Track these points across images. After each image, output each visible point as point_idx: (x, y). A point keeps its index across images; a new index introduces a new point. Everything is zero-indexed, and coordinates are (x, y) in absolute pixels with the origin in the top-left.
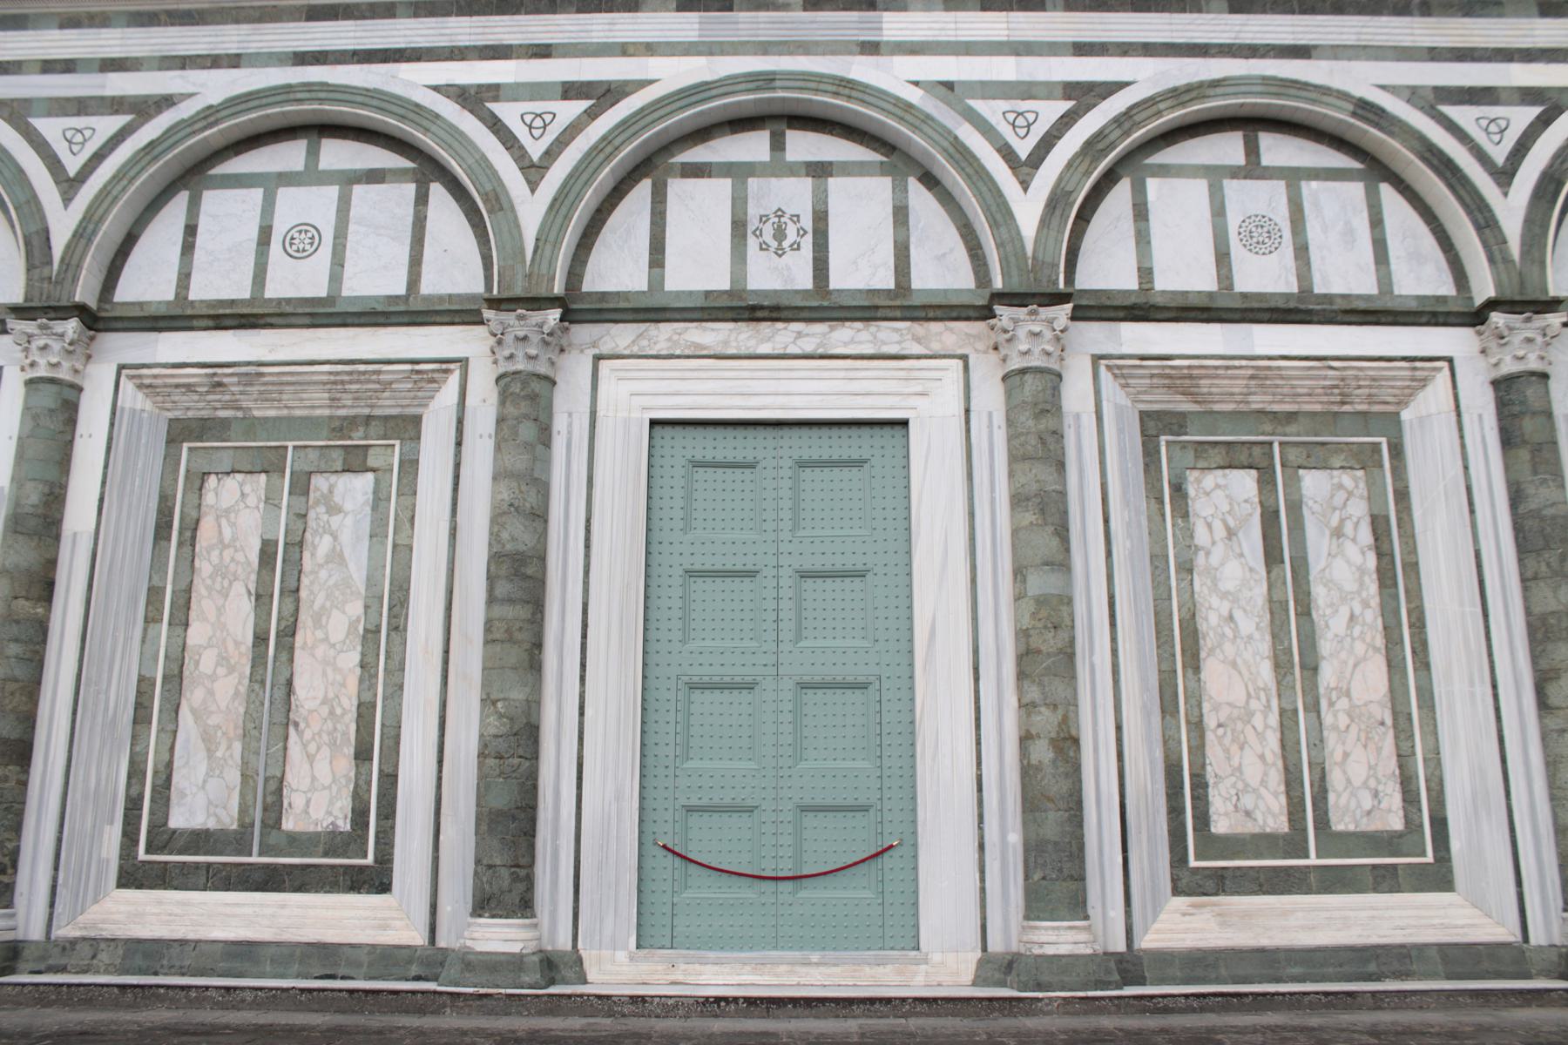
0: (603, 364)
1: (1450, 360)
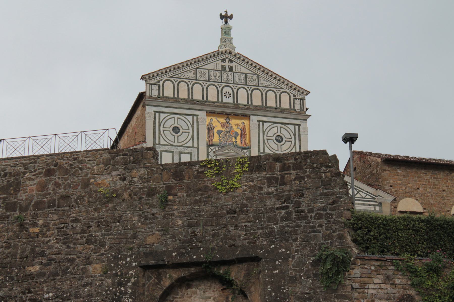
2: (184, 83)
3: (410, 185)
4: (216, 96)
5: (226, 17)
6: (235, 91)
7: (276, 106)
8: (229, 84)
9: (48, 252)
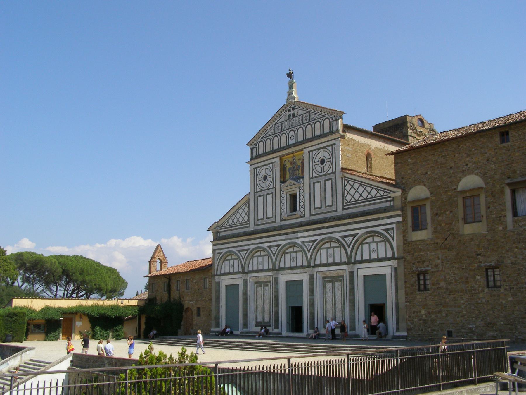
3: (419, 172)
5: (290, 75)
6: (296, 132)
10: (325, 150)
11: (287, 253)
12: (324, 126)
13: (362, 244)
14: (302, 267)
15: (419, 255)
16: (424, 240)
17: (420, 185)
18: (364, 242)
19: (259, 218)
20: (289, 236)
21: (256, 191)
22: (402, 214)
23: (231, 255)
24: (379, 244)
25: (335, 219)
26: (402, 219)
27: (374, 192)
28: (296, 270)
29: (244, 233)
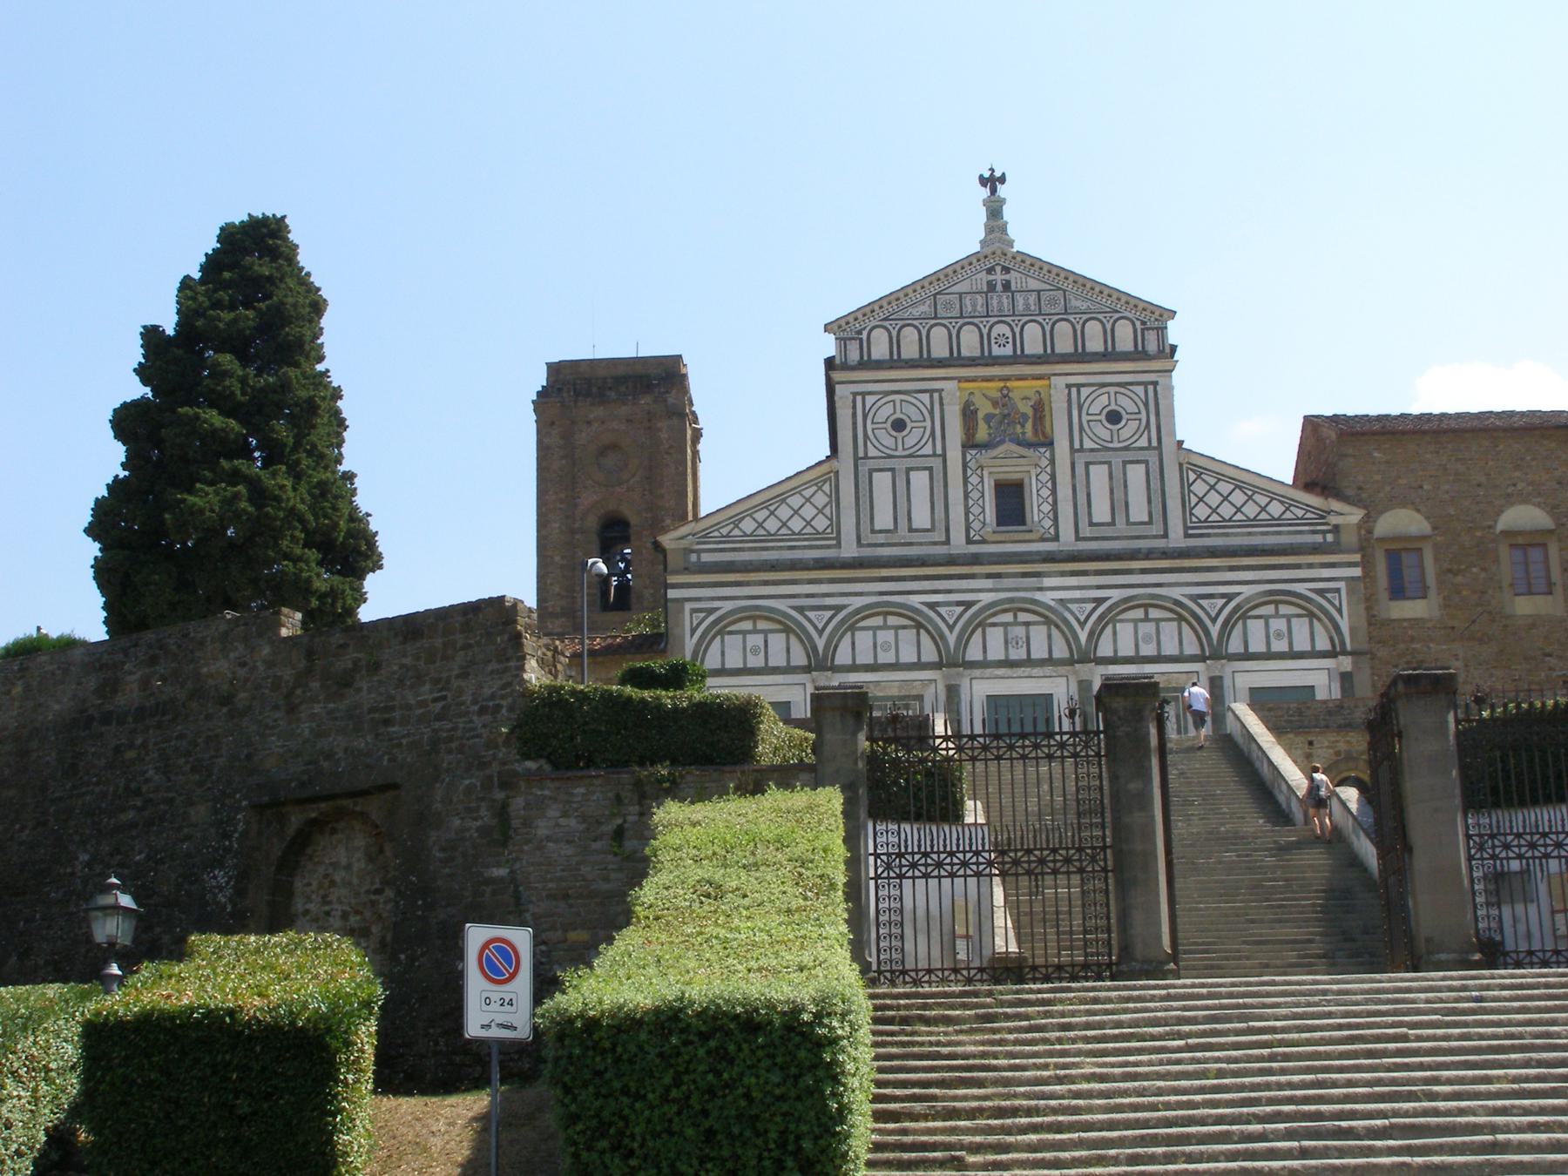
0: (973, 681)
1: (1197, 672)
2: (911, 328)
3: (1402, 481)
4: (978, 345)
5: (992, 182)
6: (1017, 330)
7: (1106, 349)
8: (1003, 319)
9: (144, 789)
10: (1122, 390)
11: (994, 625)
12: (1116, 334)
13: (1244, 617)
14: (1050, 661)
15: (1408, 650)
16: (1422, 619)
17: (1404, 507)
18: (1250, 614)
19: (877, 527)
20: (1007, 583)
21: (861, 454)
22: (1362, 562)
23: (754, 619)
24: (1294, 620)
25: (1165, 554)
26: (1363, 571)
27: (1276, 509)
28: (1029, 669)
29: (817, 561)
